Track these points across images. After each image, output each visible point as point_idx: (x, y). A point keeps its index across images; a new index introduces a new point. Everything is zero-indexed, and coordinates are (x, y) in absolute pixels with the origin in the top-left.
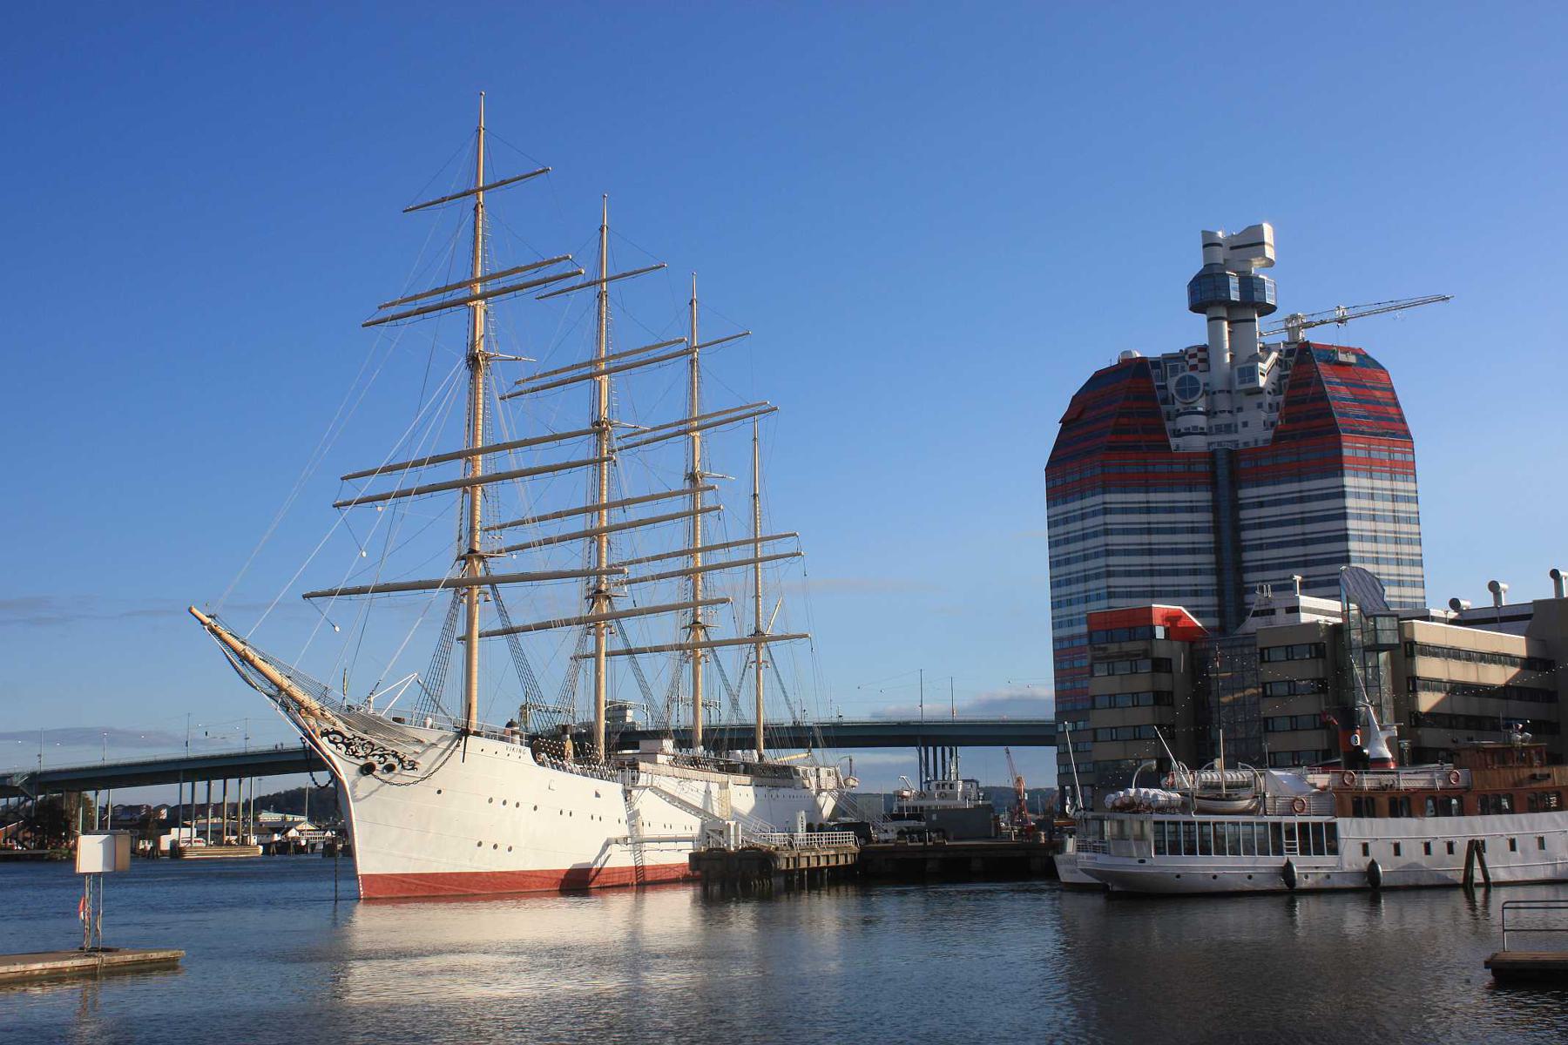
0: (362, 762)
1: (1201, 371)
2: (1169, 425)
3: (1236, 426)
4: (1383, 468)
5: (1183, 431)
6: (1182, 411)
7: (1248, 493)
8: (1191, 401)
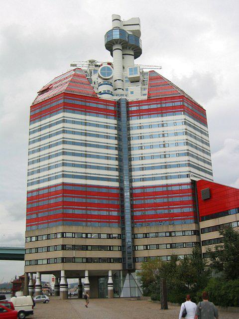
6: (102, 83)
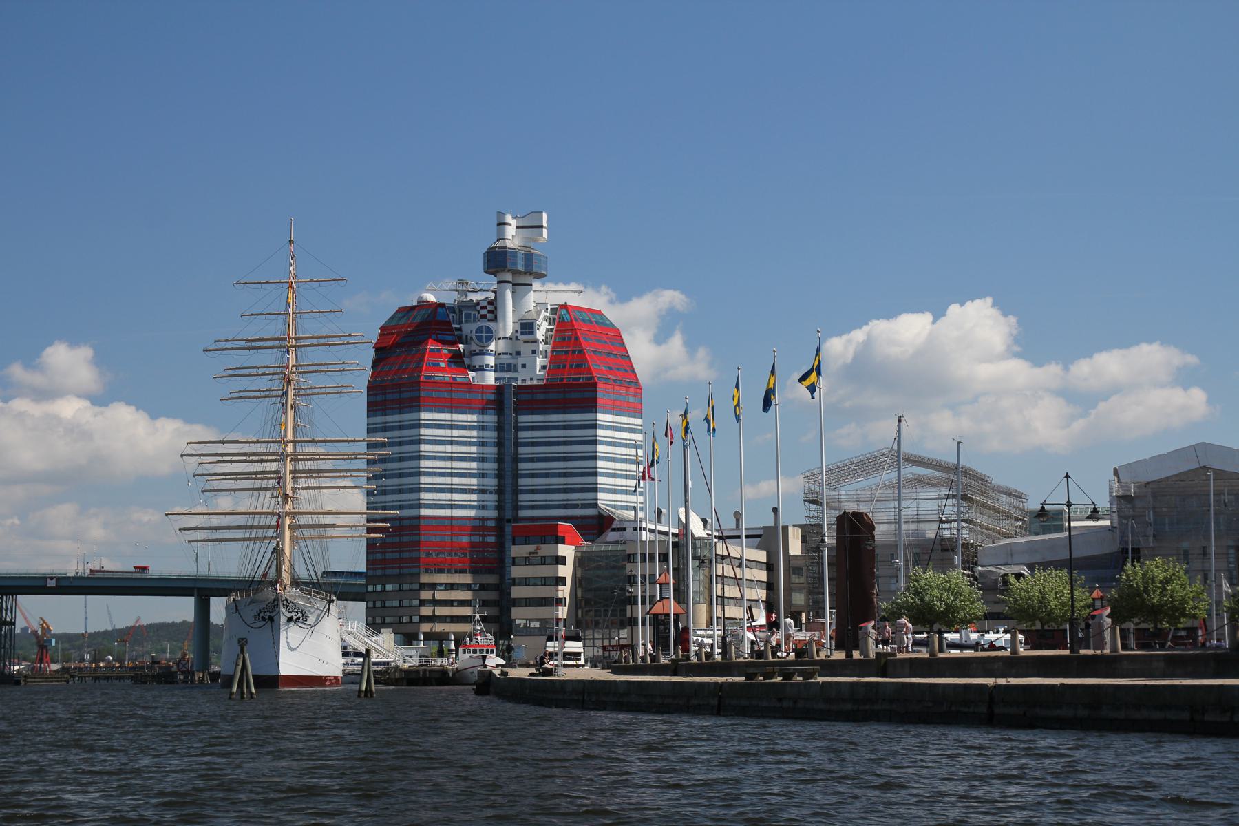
0: (289, 615)
1: (489, 321)
3: (515, 366)
5: (477, 367)
6: (477, 351)
7: (525, 419)
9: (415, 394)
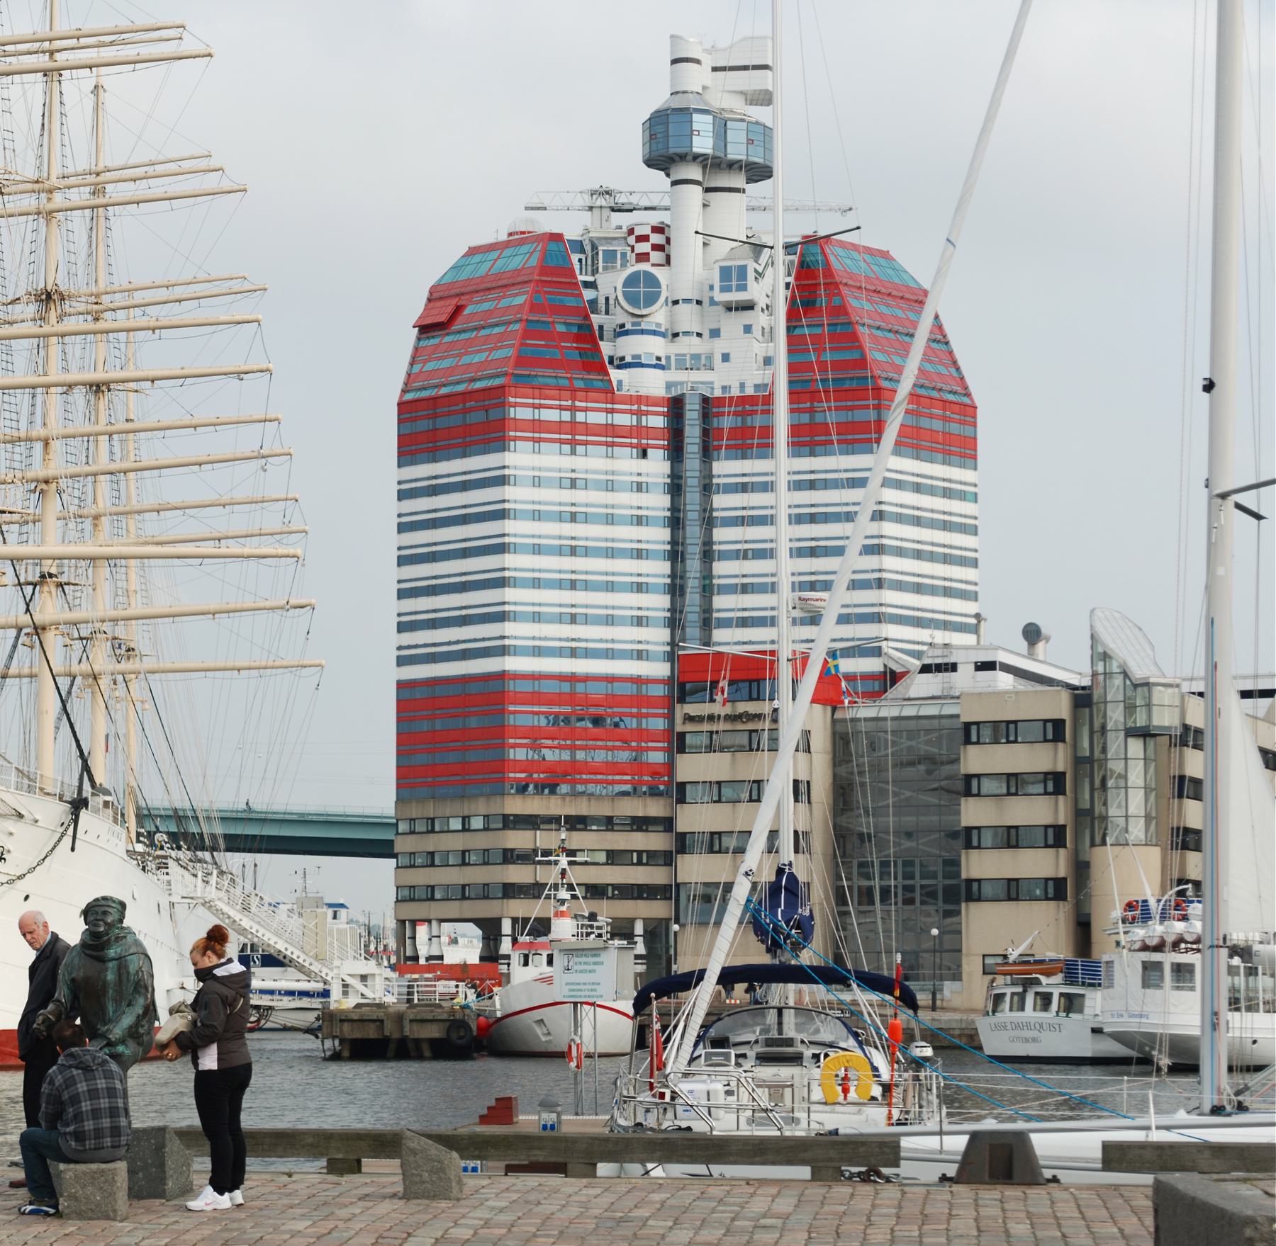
1: (653, 265)
2: (606, 348)
3: (710, 357)
4: (934, 445)
5: (628, 359)
6: (628, 327)
7: (725, 468)
8: (644, 312)
9: (494, 414)
